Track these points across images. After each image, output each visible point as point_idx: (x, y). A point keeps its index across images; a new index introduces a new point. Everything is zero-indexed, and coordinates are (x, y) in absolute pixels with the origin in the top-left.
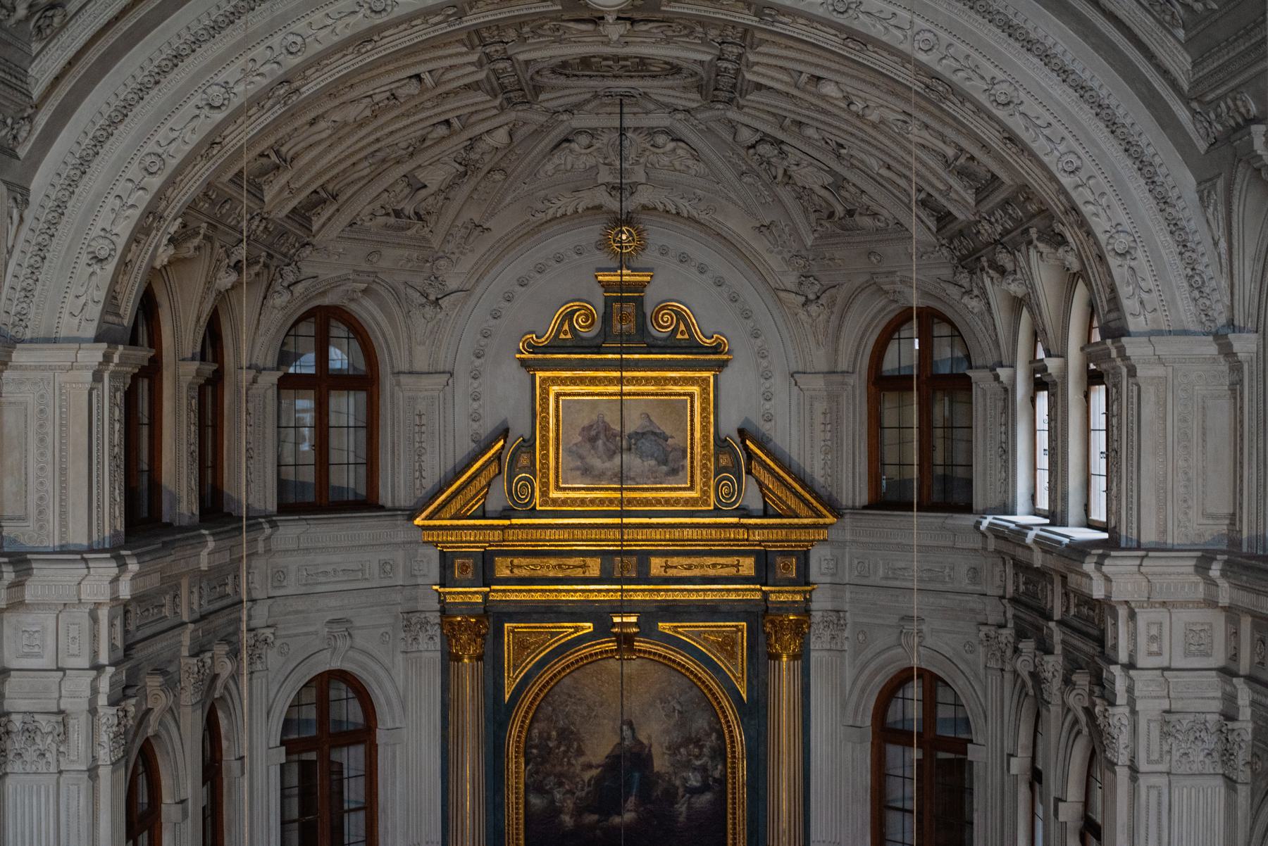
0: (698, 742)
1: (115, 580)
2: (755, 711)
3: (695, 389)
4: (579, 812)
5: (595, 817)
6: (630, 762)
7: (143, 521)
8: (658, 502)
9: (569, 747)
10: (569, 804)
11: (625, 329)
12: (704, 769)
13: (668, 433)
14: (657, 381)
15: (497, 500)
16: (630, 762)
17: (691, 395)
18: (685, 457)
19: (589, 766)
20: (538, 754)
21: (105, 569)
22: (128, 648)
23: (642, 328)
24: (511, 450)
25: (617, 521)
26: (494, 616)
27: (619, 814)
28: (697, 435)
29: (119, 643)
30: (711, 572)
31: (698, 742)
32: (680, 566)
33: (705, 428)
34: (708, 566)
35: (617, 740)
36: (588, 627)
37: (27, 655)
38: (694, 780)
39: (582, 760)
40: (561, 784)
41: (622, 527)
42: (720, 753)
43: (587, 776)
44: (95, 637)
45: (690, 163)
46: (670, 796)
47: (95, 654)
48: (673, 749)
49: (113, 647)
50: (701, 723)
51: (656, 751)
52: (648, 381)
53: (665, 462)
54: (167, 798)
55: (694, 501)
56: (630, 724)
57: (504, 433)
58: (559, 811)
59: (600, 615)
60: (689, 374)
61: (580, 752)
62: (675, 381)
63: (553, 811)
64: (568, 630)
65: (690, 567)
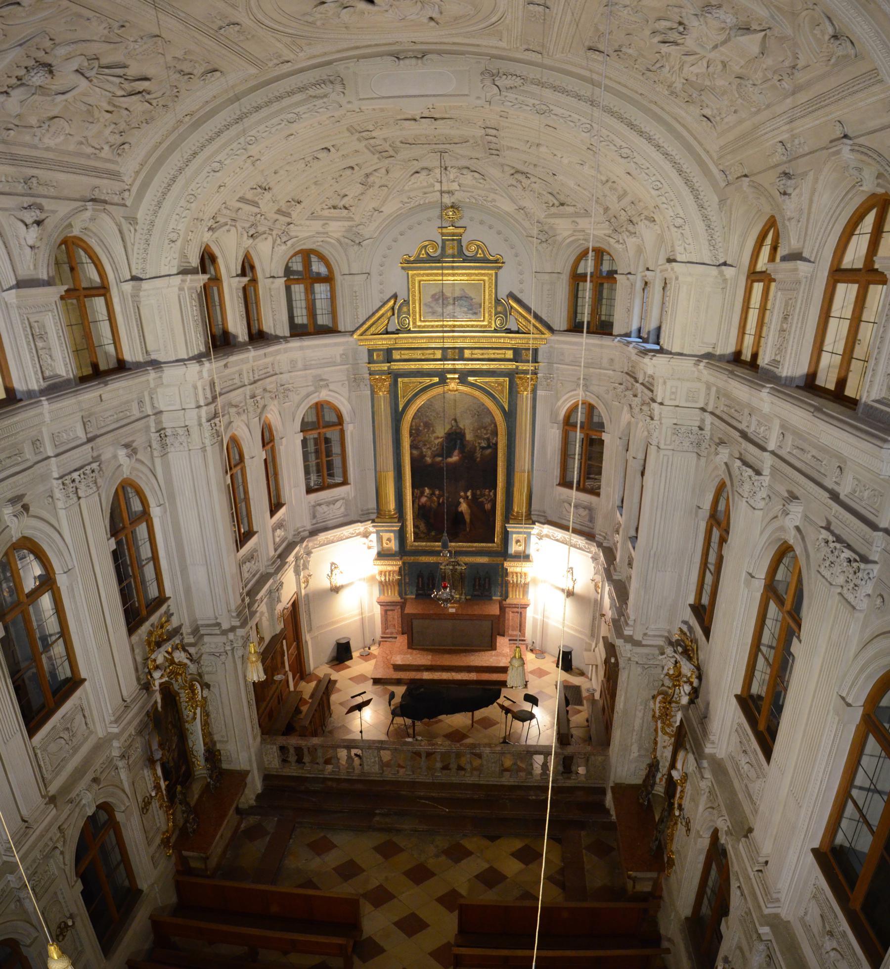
0: (485, 428)
1: (201, 372)
2: (510, 416)
3: (486, 278)
4: (434, 456)
5: (440, 459)
6: (455, 438)
7: (220, 343)
8: (468, 326)
9: (429, 429)
10: (429, 453)
11: (453, 252)
12: (488, 439)
13: (473, 296)
14: (468, 275)
15: (394, 325)
16: (455, 438)
17: (484, 281)
18: (480, 307)
19: (438, 438)
20: (415, 433)
21: (194, 367)
22: (214, 398)
23: (460, 252)
24: (399, 305)
25: (441, 334)
26: (396, 376)
27: (451, 457)
28: (487, 297)
29: (209, 396)
30: (492, 356)
31: (485, 428)
32: (478, 354)
33: (490, 295)
34: (491, 354)
35: (448, 427)
36: (436, 380)
37: (169, 405)
38: (484, 444)
39: (435, 435)
40: (425, 445)
41: (443, 337)
42: (495, 433)
43: (437, 442)
44: (196, 395)
45: (481, 181)
46: (472, 452)
47: (197, 401)
48: (475, 430)
49: (206, 398)
50: (487, 420)
51: (467, 432)
52: (463, 274)
53: (471, 310)
54: (246, 457)
55: (485, 326)
56: (455, 420)
57: (395, 296)
58: (425, 456)
59: (442, 375)
60: (483, 272)
61: (434, 432)
62: (476, 275)
63: (422, 456)
64: (427, 381)
65: (483, 354)
